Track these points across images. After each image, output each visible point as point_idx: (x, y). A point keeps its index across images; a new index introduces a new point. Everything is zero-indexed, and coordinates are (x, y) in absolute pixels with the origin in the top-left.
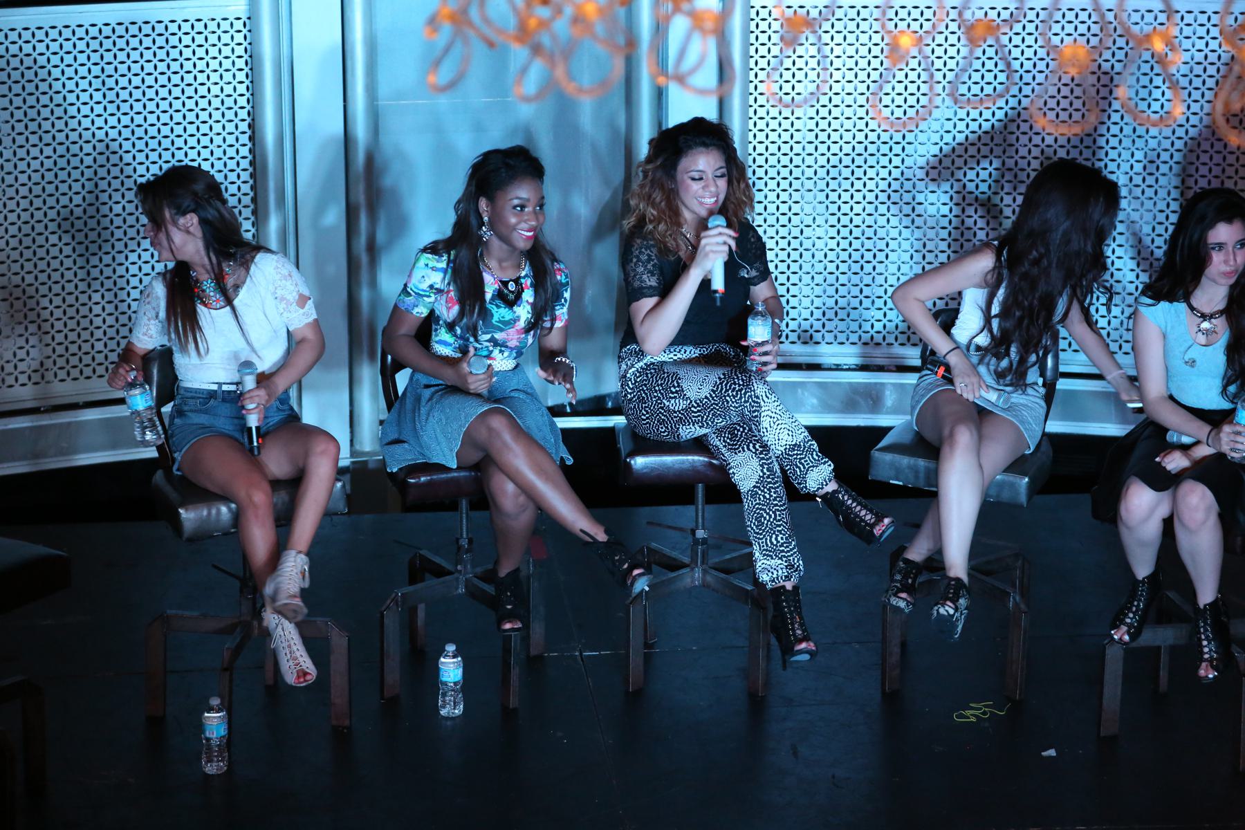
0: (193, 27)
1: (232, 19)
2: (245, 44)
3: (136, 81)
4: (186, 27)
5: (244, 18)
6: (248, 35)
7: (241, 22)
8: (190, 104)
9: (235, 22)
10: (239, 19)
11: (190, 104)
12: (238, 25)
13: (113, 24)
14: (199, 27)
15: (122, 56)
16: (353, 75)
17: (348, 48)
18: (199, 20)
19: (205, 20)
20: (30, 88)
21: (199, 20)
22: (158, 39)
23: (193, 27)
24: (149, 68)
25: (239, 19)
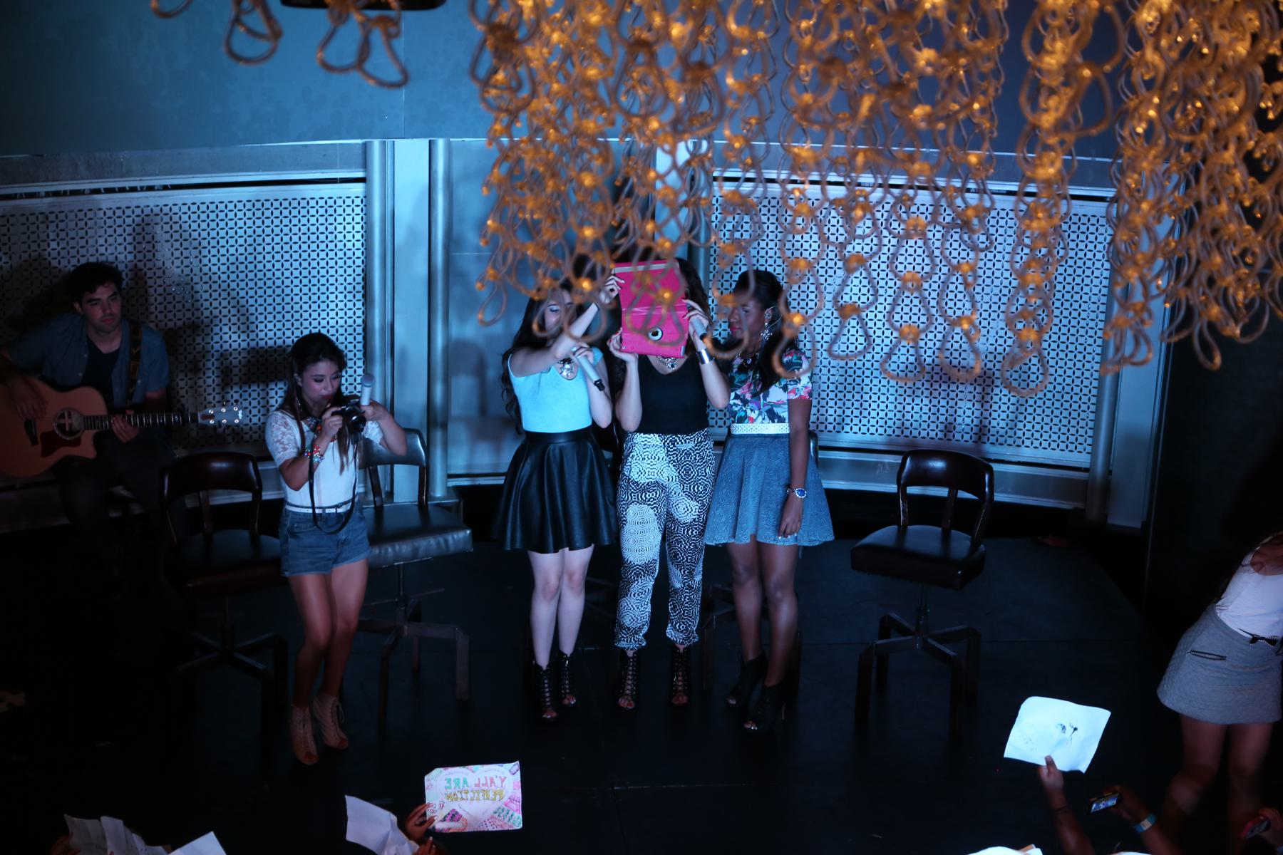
1: (353, 197)
2: (362, 214)
3: (286, 239)
5: (362, 197)
6: (364, 208)
7: (360, 199)
8: (323, 255)
9: (356, 200)
10: (357, 197)
11: (323, 255)
12: (358, 201)
13: (272, 200)
17: (432, 219)
19: (335, 198)
24: (295, 230)
25: (357, 197)
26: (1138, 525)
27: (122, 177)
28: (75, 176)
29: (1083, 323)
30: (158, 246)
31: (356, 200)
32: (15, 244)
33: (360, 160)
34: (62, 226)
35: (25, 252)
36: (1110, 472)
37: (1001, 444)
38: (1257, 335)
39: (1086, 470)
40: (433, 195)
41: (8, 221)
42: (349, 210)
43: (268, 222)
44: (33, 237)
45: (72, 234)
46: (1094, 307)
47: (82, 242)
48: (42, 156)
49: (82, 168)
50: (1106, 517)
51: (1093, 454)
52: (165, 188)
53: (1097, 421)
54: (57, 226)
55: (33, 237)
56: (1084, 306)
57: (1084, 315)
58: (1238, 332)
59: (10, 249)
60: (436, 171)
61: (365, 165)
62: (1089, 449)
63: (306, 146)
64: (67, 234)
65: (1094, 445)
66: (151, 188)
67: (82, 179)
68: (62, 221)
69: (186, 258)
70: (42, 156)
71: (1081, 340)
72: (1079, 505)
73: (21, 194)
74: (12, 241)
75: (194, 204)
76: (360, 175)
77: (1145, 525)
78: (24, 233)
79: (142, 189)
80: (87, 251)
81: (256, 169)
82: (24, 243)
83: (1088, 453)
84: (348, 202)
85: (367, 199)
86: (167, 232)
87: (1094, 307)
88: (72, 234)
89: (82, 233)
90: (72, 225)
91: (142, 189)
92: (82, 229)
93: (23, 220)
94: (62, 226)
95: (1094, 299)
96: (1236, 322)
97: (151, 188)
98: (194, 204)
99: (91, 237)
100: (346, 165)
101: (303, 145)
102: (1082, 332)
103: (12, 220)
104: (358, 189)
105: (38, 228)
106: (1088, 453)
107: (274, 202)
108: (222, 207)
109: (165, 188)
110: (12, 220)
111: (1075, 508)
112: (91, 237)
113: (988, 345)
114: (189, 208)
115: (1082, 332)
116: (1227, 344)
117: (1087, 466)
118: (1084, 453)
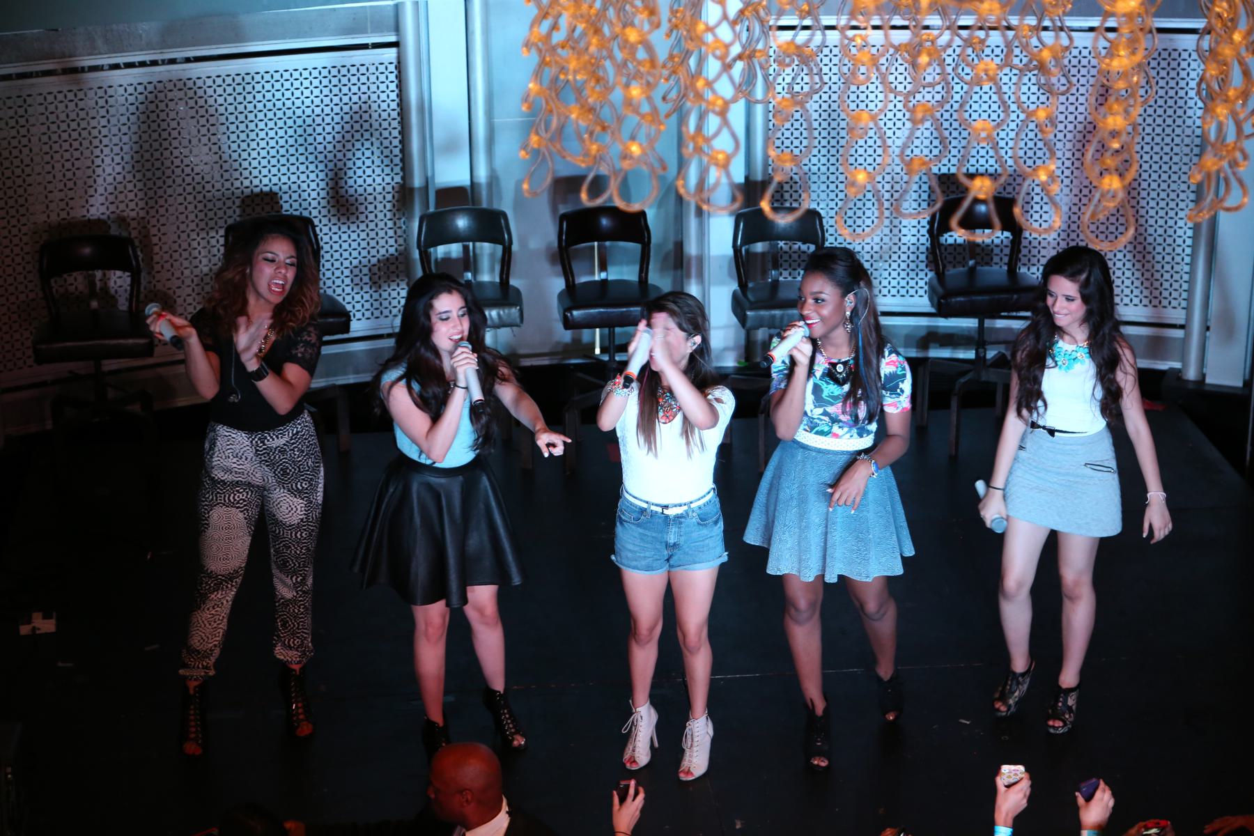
0: (358, 70)
1: (386, 64)
4: (353, 70)
5: (395, 61)
7: (393, 66)
9: (389, 66)
12: (392, 68)
13: (301, 70)
14: (363, 70)
15: (307, 93)
16: (476, 103)
17: (471, 83)
18: (363, 65)
20: (241, 117)
21: (363, 65)
22: (333, 79)
23: (358, 70)
26: (1240, 384)
27: (142, 50)
28: (93, 51)
29: (1175, 168)
30: (183, 123)
31: (389, 66)
32: (34, 125)
33: (392, 22)
34: (81, 104)
35: (45, 134)
36: (1208, 329)
39: (1182, 327)
40: (471, 57)
41: (25, 101)
42: (382, 78)
43: (297, 93)
44: (53, 117)
45: (92, 113)
46: (1187, 150)
47: (104, 122)
48: (57, 30)
49: (99, 42)
50: (1204, 376)
52: (188, 60)
54: (77, 105)
55: (53, 117)
56: (1176, 149)
57: (1176, 159)
59: (28, 131)
60: (473, 33)
61: (397, 28)
62: (1184, 304)
63: (334, 9)
64: (87, 114)
66: (173, 61)
67: (101, 54)
68: (81, 100)
69: (214, 134)
70: (57, 30)
71: (1173, 186)
72: (1177, 365)
73: (37, 72)
74: (30, 123)
75: (219, 76)
76: (393, 39)
77: (1247, 384)
78: (43, 114)
79: (164, 62)
80: (110, 130)
81: (283, 37)
82: (43, 124)
84: (382, 68)
85: (400, 66)
86: (192, 108)
87: (1187, 150)
88: (92, 113)
89: (103, 112)
90: (92, 103)
91: (164, 62)
92: (103, 107)
93: (40, 99)
94: (81, 104)
95: (1187, 141)
97: (173, 61)
98: (219, 76)
99: (113, 116)
100: (377, 29)
101: (330, 9)
102: (1175, 177)
103: (29, 100)
104: (391, 53)
105: (57, 108)
107: (303, 72)
108: (248, 79)
109: (188, 60)
110: (29, 100)
111: (1172, 370)
112: (113, 116)
113: (1071, 196)
114: (214, 82)
115: (1175, 177)
117: (1183, 322)
118: (1179, 308)
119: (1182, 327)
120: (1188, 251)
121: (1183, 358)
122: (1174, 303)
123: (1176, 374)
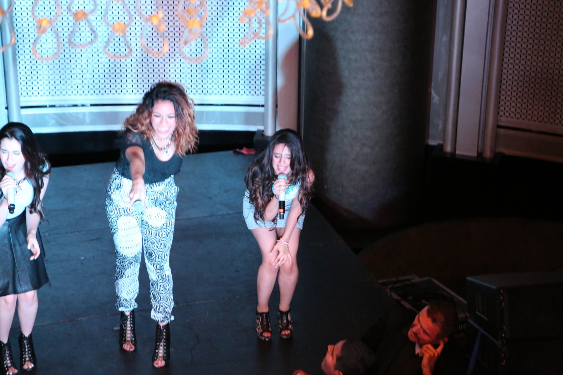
36: (277, 106)
37: (210, 94)
38: (335, 15)
39: (263, 106)
51: (266, 96)
53: (266, 75)
58: (324, 13)
62: (263, 93)
65: (266, 90)
72: (261, 128)
83: (263, 95)
96: (322, 7)
106: (263, 95)
116: (316, 22)
117: (263, 103)
118: (261, 96)
119: (263, 106)
120: (263, 62)
121: (264, 123)
122: (258, 92)
123: (261, 133)
